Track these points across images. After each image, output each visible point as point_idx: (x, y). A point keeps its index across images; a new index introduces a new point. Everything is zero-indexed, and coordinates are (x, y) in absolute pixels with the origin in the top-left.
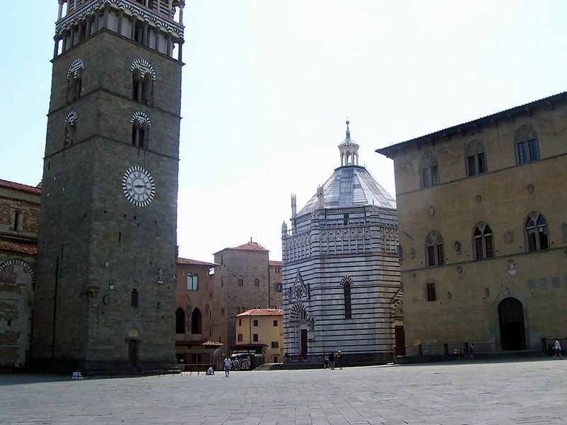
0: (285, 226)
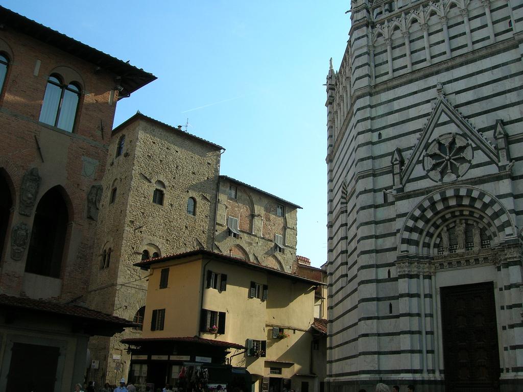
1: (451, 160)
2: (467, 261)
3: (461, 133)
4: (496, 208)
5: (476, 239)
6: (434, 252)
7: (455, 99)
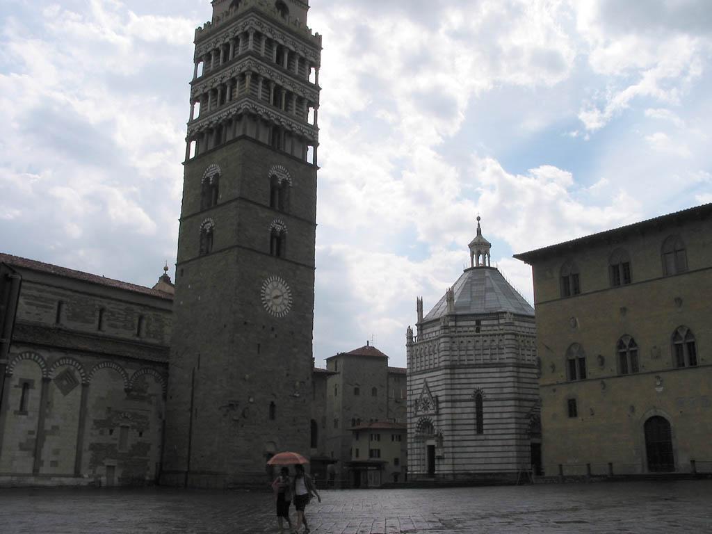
0: (410, 331)
6: (425, 434)
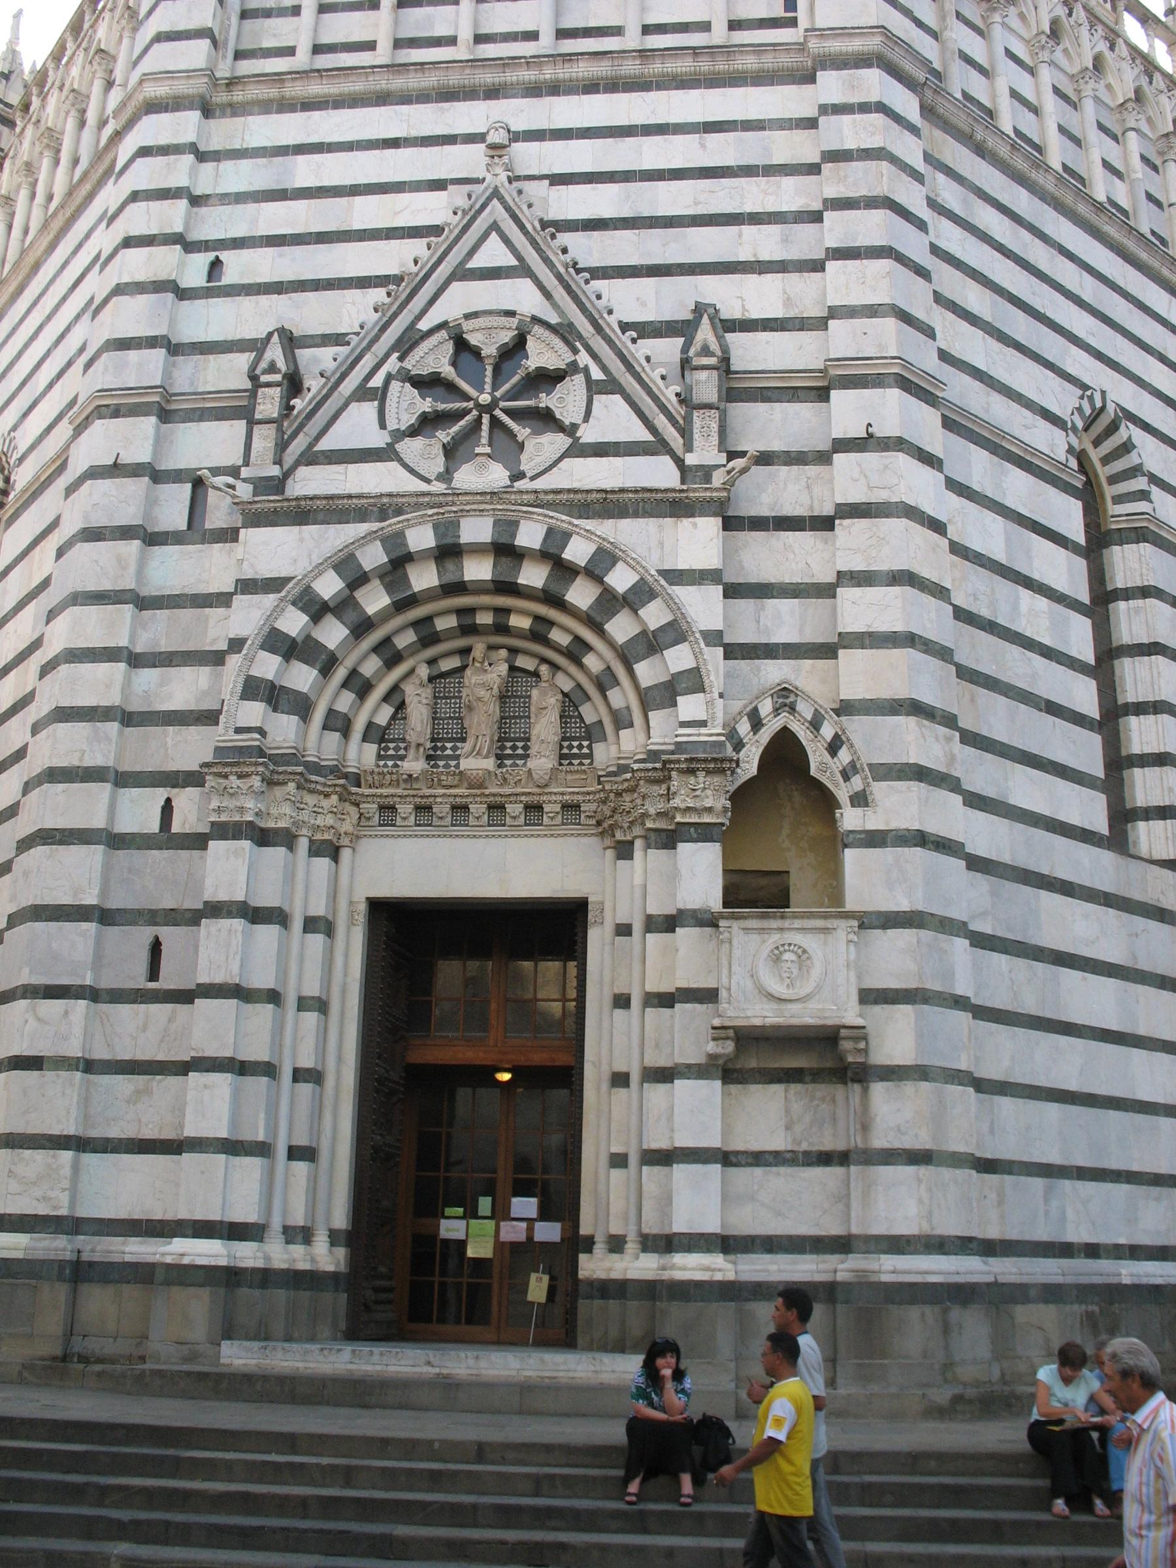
1: (498, 412)
2: (496, 808)
3: (554, 319)
4: (654, 615)
5: (545, 728)
6: (362, 755)
7: (545, 200)
